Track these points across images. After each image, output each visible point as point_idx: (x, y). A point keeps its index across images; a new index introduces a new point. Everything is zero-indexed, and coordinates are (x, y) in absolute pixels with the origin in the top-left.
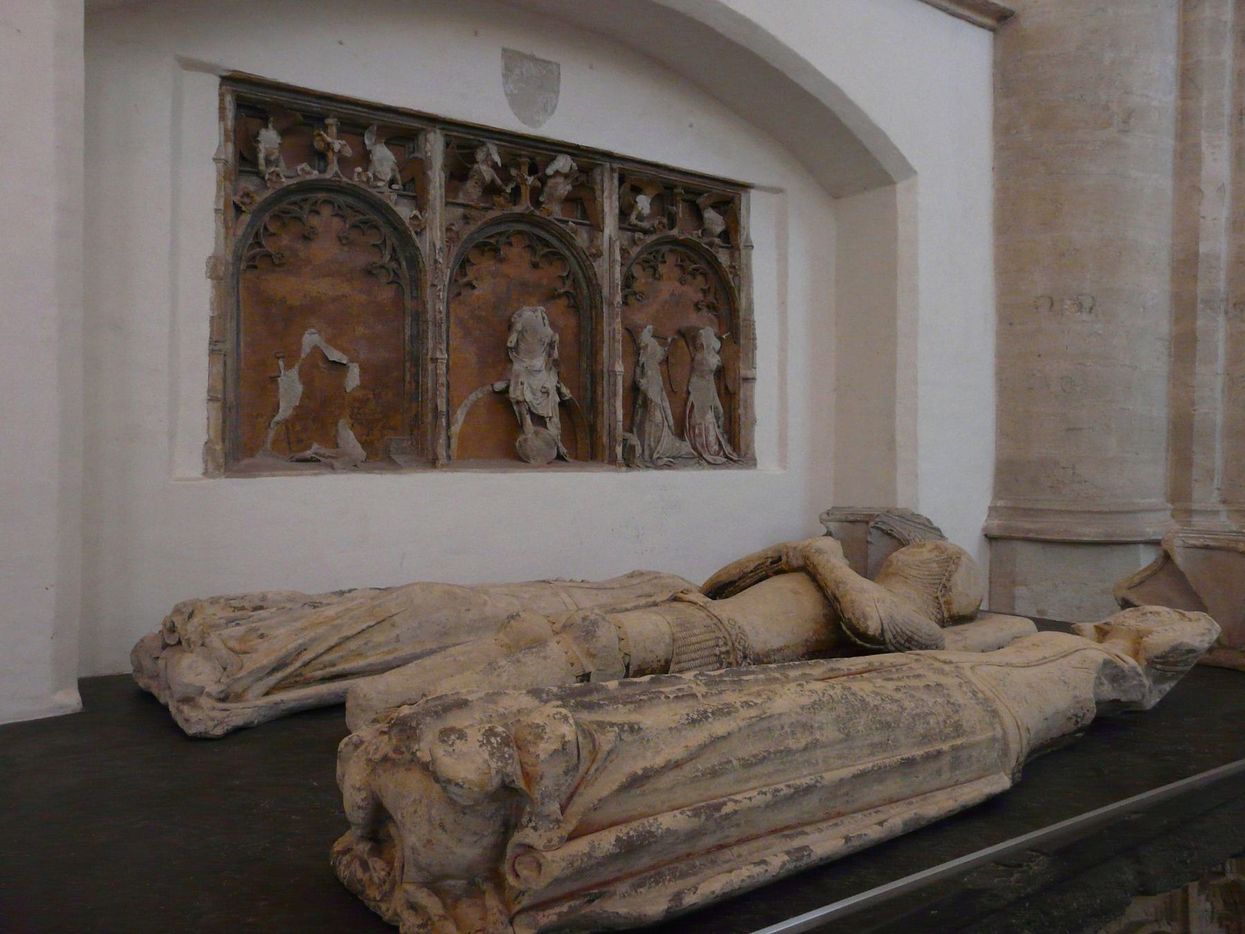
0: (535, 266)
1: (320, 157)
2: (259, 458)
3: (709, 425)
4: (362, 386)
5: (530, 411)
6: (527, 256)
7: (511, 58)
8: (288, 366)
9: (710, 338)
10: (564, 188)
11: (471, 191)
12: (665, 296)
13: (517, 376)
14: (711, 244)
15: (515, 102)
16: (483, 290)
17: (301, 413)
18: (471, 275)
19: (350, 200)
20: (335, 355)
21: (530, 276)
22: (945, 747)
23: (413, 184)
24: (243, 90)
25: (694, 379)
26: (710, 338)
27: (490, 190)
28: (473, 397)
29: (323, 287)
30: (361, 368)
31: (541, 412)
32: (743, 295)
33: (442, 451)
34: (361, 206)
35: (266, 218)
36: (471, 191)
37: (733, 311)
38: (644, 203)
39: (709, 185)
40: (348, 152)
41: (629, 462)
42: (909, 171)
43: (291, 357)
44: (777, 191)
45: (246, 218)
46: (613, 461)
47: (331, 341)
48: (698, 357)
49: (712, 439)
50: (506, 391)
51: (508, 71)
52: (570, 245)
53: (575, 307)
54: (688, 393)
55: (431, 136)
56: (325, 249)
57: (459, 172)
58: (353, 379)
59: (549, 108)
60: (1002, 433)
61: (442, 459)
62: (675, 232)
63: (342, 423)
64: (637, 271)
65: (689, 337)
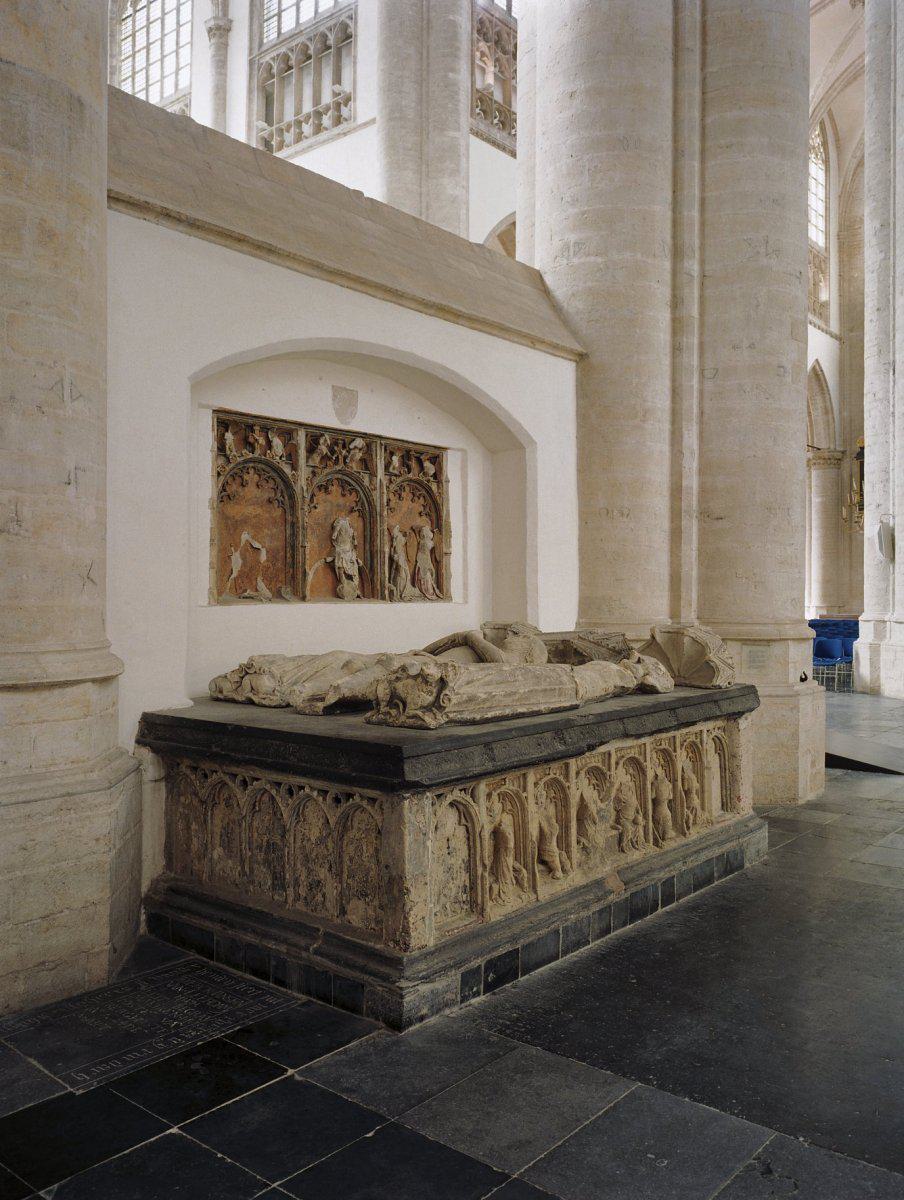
0: (344, 495)
1: (251, 447)
3: (429, 580)
4: (267, 561)
5: (345, 573)
7: (337, 391)
10: (359, 455)
11: (316, 458)
12: (404, 509)
13: (339, 555)
14: (428, 481)
15: (338, 414)
17: (241, 574)
19: (263, 466)
20: (257, 545)
22: (557, 687)
23: (291, 457)
24: (221, 415)
25: (419, 554)
26: (427, 531)
27: (324, 458)
29: (250, 510)
30: (267, 552)
31: (350, 572)
33: (308, 593)
34: (268, 469)
36: (316, 458)
37: (439, 518)
38: (396, 460)
41: (391, 600)
42: (533, 443)
46: (383, 598)
48: (422, 542)
49: (430, 587)
50: (333, 561)
51: (335, 396)
52: (361, 484)
53: (362, 515)
54: (416, 561)
56: (251, 491)
58: (263, 557)
59: (353, 415)
60: (582, 583)
61: (308, 597)
62: (410, 476)
63: (259, 579)
65: (417, 531)
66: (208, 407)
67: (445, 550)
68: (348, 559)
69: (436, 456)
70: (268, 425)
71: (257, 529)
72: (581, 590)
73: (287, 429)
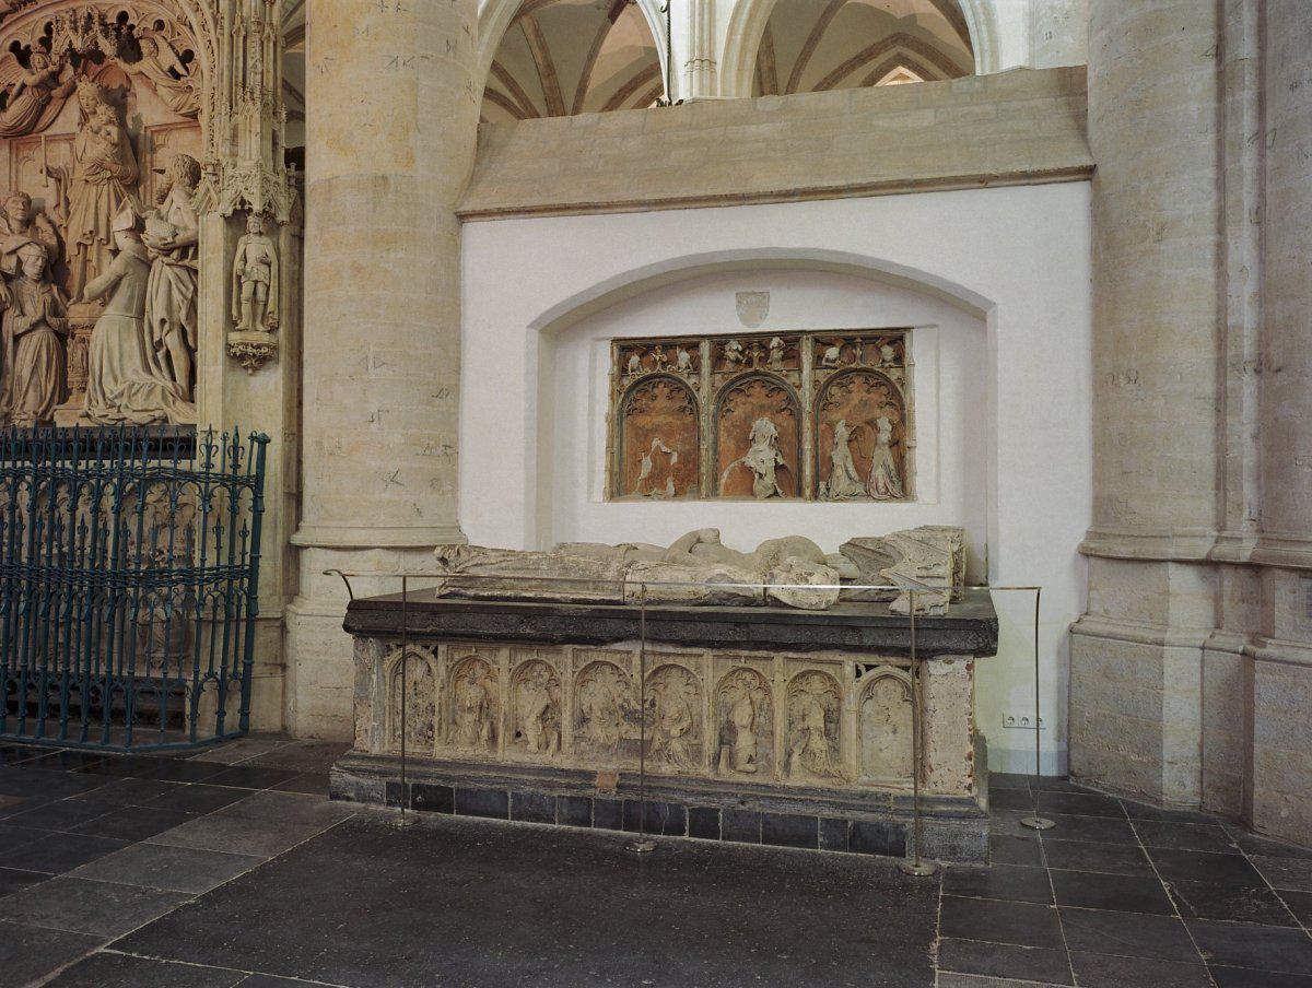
2: (634, 494)
4: (679, 462)
6: (764, 392)
8: (646, 455)
9: (884, 424)
10: (776, 354)
11: (729, 366)
15: (743, 319)
16: (739, 412)
17: (651, 476)
18: (730, 406)
20: (665, 449)
21: (766, 401)
23: (695, 367)
24: (620, 343)
26: (884, 424)
27: (737, 361)
28: (732, 465)
29: (661, 419)
30: (679, 455)
32: (907, 395)
33: (704, 492)
35: (634, 393)
37: (902, 408)
39: (877, 333)
40: (665, 359)
41: (815, 496)
43: (647, 451)
44: (935, 326)
45: (623, 395)
47: (665, 443)
49: (881, 484)
55: (702, 344)
56: (662, 402)
57: (718, 359)
58: (674, 459)
64: (834, 390)
65: (872, 423)
66: (603, 339)
67: (908, 443)
68: (762, 457)
69: (897, 338)
70: (670, 344)
71: (668, 435)
72: (1094, 488)
73: (691, 343)
